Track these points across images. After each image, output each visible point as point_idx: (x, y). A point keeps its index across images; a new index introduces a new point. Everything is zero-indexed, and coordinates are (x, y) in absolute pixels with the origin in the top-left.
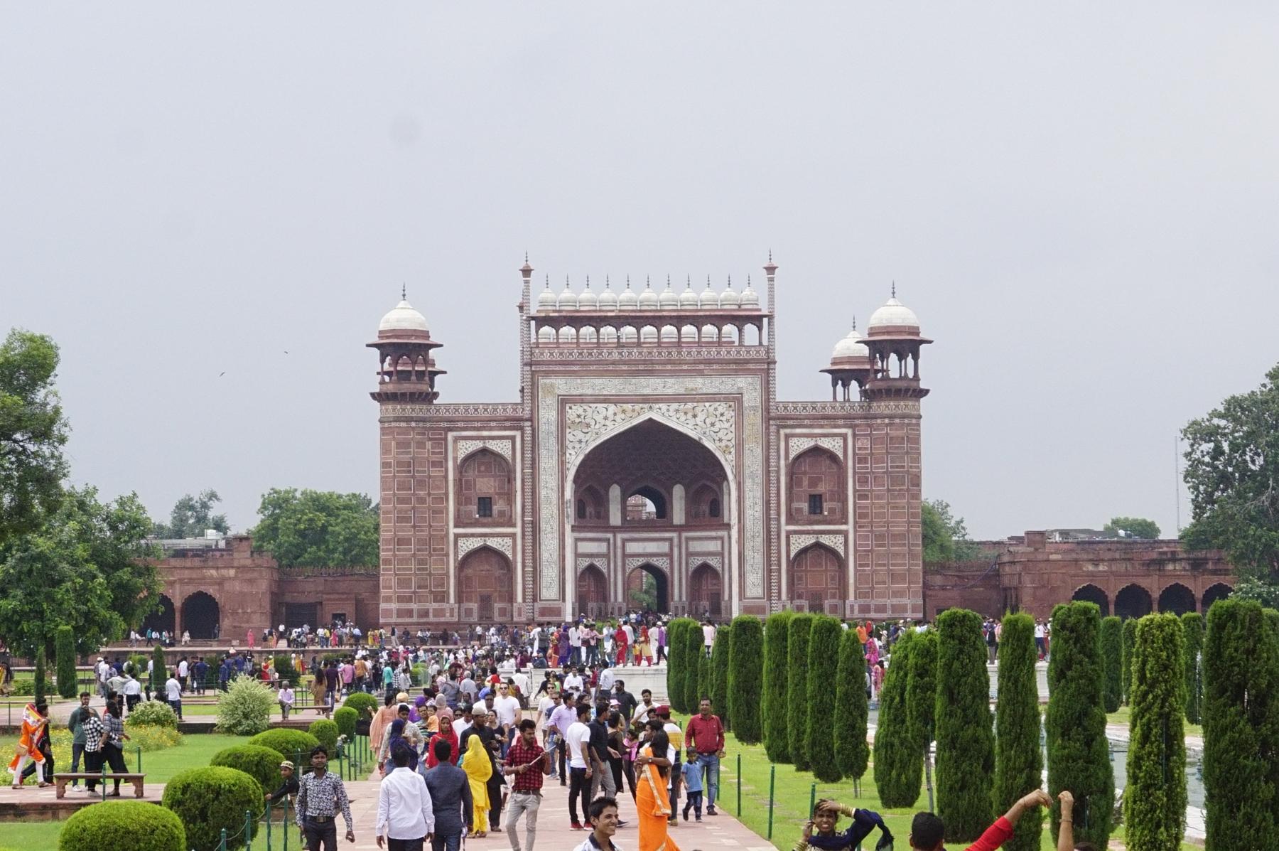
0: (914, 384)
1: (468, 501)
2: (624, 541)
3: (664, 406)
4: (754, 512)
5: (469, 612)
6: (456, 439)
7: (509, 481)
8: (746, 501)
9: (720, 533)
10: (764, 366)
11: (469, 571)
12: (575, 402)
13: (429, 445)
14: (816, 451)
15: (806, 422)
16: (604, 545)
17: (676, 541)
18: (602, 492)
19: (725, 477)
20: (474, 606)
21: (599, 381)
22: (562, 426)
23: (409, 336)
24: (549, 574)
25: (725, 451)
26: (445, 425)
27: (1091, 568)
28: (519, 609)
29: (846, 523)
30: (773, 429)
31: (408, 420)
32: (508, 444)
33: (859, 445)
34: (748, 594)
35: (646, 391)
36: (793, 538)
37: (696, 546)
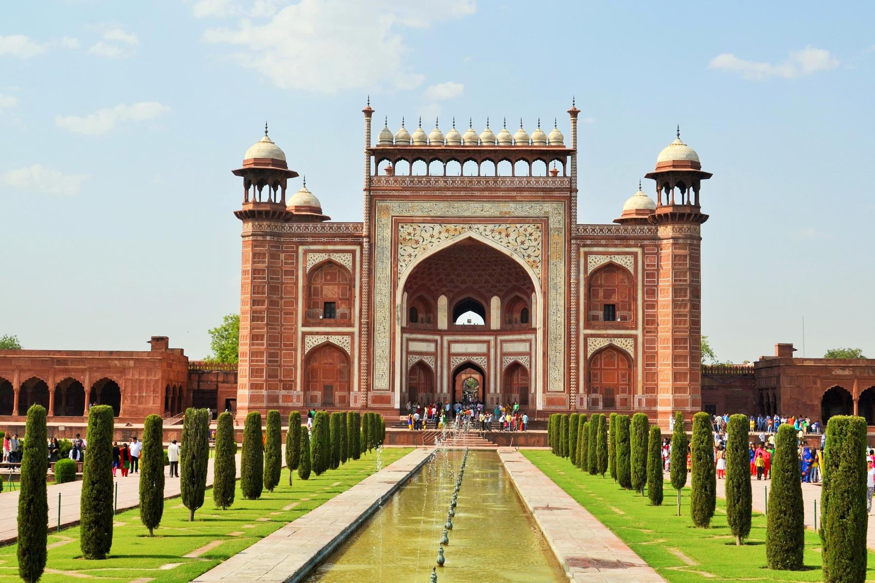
0: (695, 210)
1: (316, 305)
2: (450, 342)
3: (481, 227)
4: (558, 319)
5: (313, 399)
6: (306, 252)
7: (350, 289)
9: (529, 336)
10: (567, 194)
11: (315, 364)
12: (406, 223)
13: (282, 256)
14: (611, 267)
15: (603, 242)
16: (433, 345)
17: (492, 343)
18: (432, 301)
19: (533, 290)
20: (319, 394)
21: (427, 205)
22: (396, 243)
23: (268, 164)
24: (381, 367)
25: (533, 265)
26: (295, 240)
27: (840, 372)
28: (356, 398)
29: (636, 328)
30: (573, 247)
31: (265, 234)
32: (349, 256)
33: (647, 262)
34: (551, 388)
35: (467, 214)
36: (590, 341)
37: (509, 348)
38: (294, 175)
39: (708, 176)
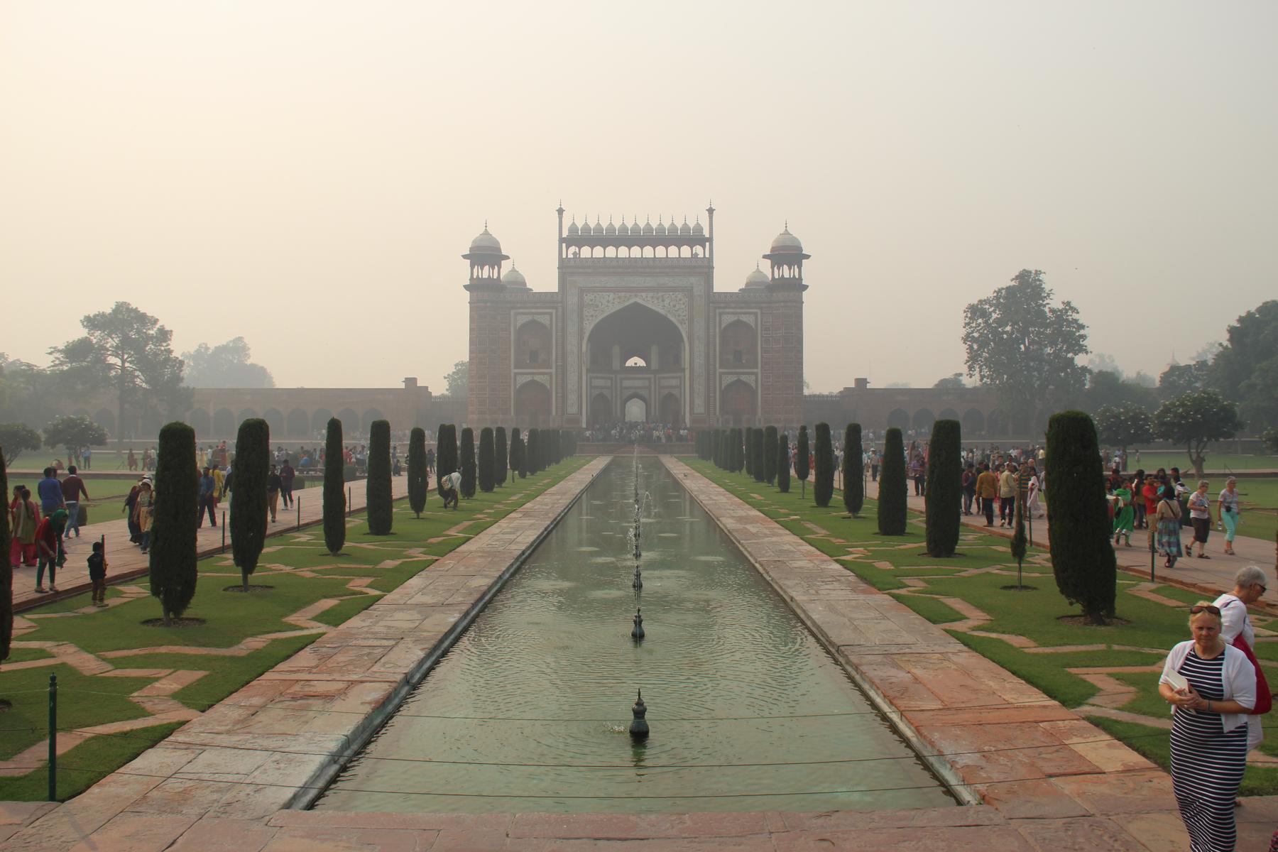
4: (699, 361)
8: (694, 355)
14: (738, 324)
24: (572, 397)
32: (548, 317)
38: (507, 258)
39: (808, 257)
